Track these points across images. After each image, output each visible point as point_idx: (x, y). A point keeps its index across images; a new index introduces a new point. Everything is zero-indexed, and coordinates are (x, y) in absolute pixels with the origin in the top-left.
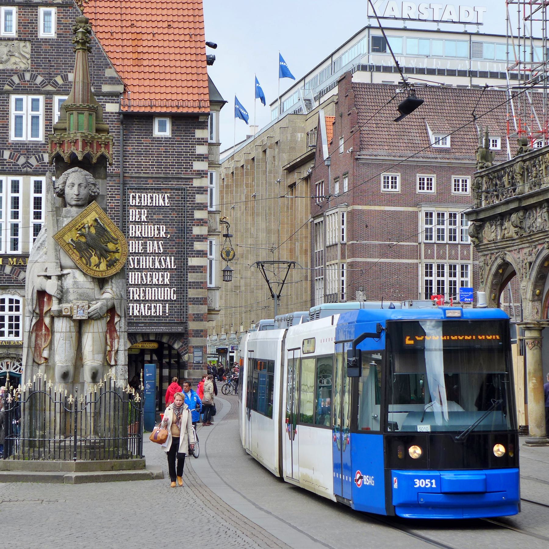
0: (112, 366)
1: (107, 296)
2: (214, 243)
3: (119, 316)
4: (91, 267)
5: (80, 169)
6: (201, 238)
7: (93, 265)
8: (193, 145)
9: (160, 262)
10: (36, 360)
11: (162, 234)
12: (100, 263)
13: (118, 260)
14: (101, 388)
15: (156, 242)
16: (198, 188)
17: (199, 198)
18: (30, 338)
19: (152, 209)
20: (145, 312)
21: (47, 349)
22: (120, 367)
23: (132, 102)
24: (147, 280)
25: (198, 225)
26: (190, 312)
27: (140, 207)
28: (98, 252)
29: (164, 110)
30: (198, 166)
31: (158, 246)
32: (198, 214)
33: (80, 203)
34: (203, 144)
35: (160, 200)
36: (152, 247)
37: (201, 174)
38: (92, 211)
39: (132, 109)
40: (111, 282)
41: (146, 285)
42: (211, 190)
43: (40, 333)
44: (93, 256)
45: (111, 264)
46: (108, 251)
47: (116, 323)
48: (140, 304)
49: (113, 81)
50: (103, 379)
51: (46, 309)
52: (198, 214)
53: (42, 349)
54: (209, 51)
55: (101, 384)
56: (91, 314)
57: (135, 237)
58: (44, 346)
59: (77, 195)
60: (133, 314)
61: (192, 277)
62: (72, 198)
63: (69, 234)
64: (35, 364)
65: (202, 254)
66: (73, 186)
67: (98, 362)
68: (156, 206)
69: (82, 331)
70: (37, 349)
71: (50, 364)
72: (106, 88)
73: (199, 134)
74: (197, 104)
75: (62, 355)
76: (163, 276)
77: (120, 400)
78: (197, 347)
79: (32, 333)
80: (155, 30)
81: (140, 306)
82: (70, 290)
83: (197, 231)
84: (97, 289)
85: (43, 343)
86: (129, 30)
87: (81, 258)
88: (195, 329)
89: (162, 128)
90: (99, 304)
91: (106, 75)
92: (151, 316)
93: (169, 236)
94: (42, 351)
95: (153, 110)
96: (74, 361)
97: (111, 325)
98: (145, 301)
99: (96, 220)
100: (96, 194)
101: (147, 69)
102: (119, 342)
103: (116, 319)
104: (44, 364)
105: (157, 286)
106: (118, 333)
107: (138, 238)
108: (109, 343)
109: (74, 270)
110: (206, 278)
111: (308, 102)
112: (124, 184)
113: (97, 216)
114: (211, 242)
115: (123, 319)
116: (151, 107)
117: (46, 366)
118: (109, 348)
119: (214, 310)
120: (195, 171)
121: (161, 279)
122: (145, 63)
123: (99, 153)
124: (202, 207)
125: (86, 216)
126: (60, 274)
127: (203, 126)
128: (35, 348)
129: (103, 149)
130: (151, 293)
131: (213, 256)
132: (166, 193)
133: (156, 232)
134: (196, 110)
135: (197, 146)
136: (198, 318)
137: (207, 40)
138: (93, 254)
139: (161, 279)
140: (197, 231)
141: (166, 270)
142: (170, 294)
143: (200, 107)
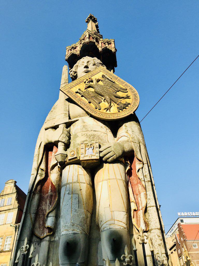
7: (102, 108)
10: (37, 232)
12: (110, 106)
21: (52, 214)
28: (107, 97)
50: (131, 247)
58: (48, 211)
67: (121, 224)
71: (57, 238)
79: (34, 194)
82: (78, 134)
84: (110, 134)
87: (90, 103)
94: (46, 218)
96: (86, 227)
99: (103, 76)
104: (48, 238)
117: (50, 242)
126: (67, 120)
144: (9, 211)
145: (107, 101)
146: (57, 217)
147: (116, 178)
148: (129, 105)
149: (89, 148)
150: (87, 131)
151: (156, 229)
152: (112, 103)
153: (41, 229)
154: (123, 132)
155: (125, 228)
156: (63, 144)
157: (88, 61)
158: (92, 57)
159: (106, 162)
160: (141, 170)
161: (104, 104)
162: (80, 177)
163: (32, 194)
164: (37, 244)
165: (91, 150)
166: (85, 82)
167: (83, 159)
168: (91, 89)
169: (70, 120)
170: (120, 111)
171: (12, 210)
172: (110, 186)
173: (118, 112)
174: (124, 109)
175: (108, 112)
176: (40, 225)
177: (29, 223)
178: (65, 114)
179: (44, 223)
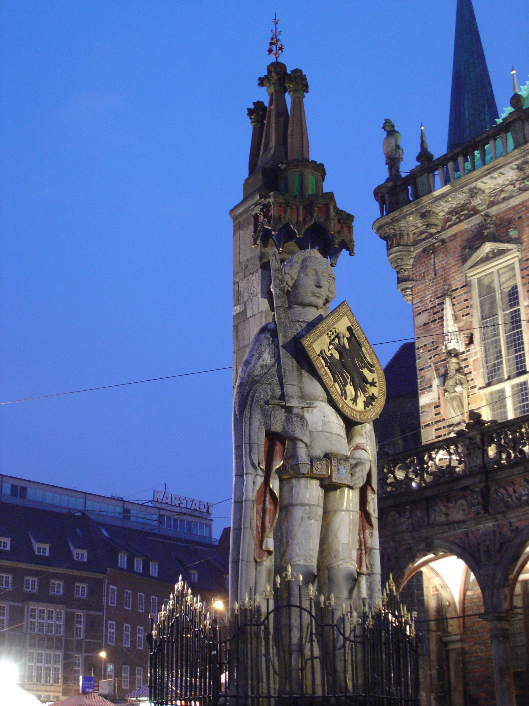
4: (347, 401)
13: (376, 398)
99: (349, 329)
102: (371, 534)
138: (349, 381)
161: (350, 389)
166: (330, 337)
170: (367, 409)
174: (370, 406)
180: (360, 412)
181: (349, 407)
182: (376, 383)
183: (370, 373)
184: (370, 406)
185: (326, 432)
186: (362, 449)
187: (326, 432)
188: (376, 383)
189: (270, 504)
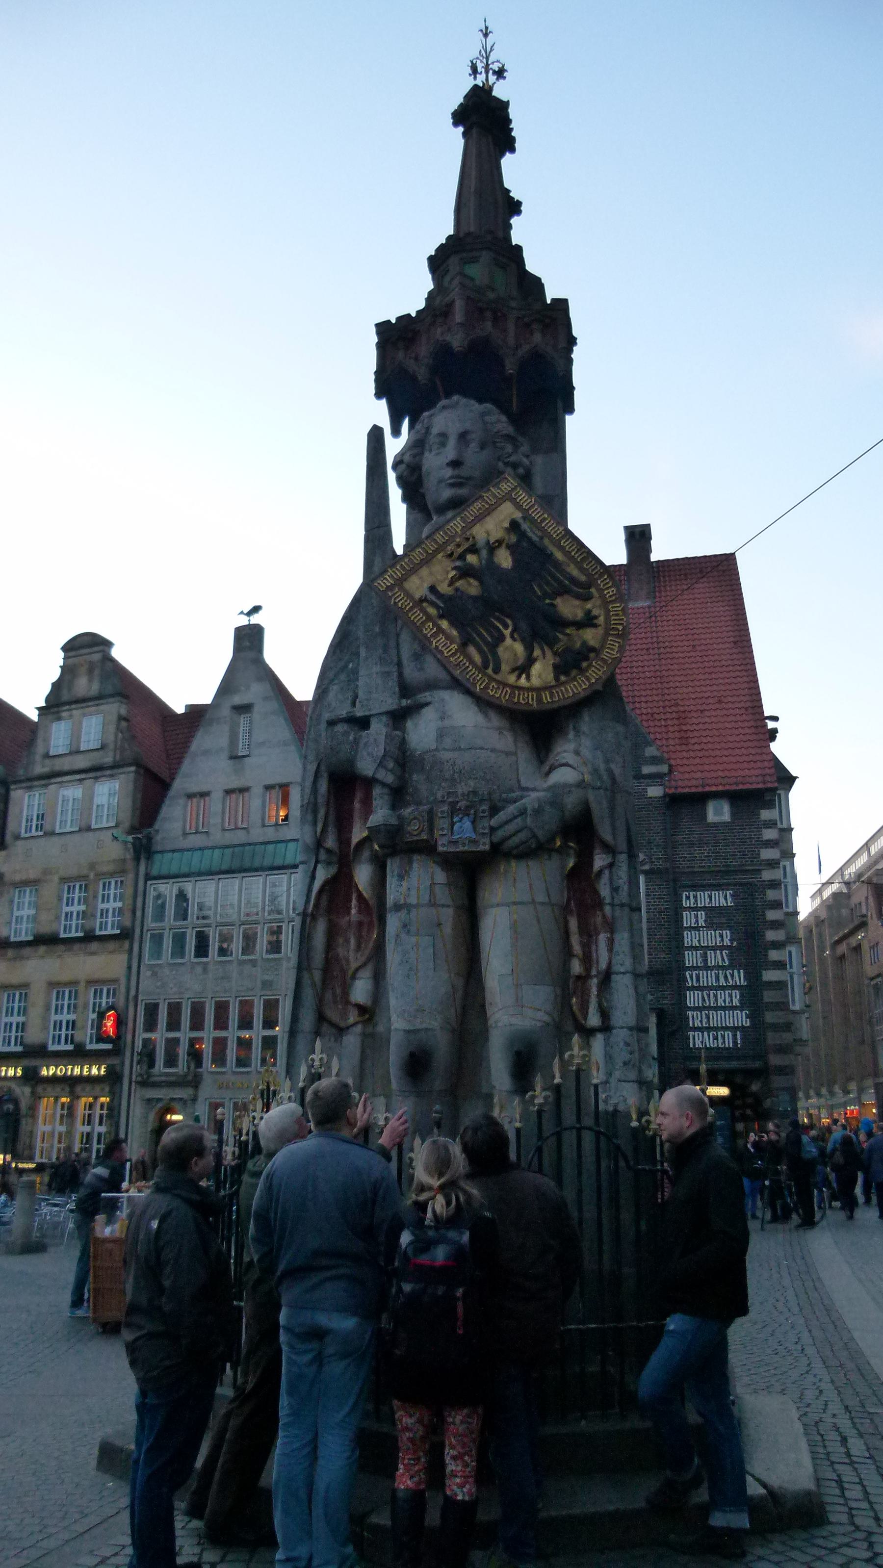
0: (588, 1033)
1: (563, 776)
2: (794, 954)
3: (609, 849)
4: (498, 677)
5: (464, 401)
6: (777, 945)
7: (505, 668)
8: (759, 829)
9: (726, 977)
11: (727, 942)
12: (530, 661)
13: (592, 649)
14: (540, 1113)
15: (718, 952)
16: (769, 881)
17: (771, 895)
18: (305, 938)
19: (711, 911)
20: (710, 1043)
22: (620, 1035)
23: (680, 783)
24: (709, 1000)
25: (772, 929)
26: (770, 1042)
27: (696, 909)
28: (523, 626)
29: (720, 788)
30: (767, 854)
31: (722, 957)
32: (772, 915)
33: (463, 492)
34: (771, 828)
35: (722, 899)
36: (714, 959)
37: (773, 864)
38: (500, 501)
39: (680, 790)
40: (575, 728)
41: (710, 1008)
42: (786, 886)
43: (343, 921)
44: (508, 641)
45: (570, 663)
46: (562, 623)
47: (600, 872)
48: (702, 1032)
49: (655, 760)
51: (358, 834)
52: (772, 915)
53: (350, 972)
54: (771, 725)
55: (540, 1095)
56: (500, 834)
57: (692, 947)
58: (354, 965)
59: (455, 464)
60: (694, 1045)
61: (769, 996)
62: (440, 481)
63: (424, 571)
64: (325, 1028)
65: (780, 965)
66: (443, 444)
68: (716, 907)
69: (479, 903)
70: (334, 976)
72: (646, 770)
73: (766, 815)
74: (760, 779)
75: (411, 991)
76: (731, 996)
77: (622, 1164)
78: (784, 1089)
79: (314, 917)
80: (705, 707)
81: (703, 1036)
83: (771, 935)
84: (524, 756)
85: (352, 955)
86: (674, 709)
88: (778, 1064)
89: (718, 812)
90: (531, 800)
91: (647, 755)
92: (718, 1048)
93: (735, 944)
95: (707, 789)
97: (580, 880)
98: (709, 1029)
99: (514, 526)
100: (521, 471)
101: (697, 747)
103: (599, 861)
104: (359, 1028)
105: (724, 1008)
106: (607, 909)
107: (696, 948)
108: (577, 948)
109: (445, 695)
110: (787, 996)
111: (847, 884)
112: (675, 880)
113: (518, 515)
114: (790, 953)
115: (623, 858)
116: (703, 786)
117: (364, 1035)
118: (576, 967)
119: (801, 1040)
120: (763, 860)
121: (728, 1000)
122: (692, 741)
123: (526, 348)
124: (777, 905)
125: (480, 518)
127: (770, 805)
128: (326, 970)
129: (537, 337)
130: (716, 1019)
131: (794, 970)
132: (728, 890)
133: (719, 939)
134: (761, 786)
135: (764, 831)
136: (782, 1050)
137: (766, 714)
138: (507, 633)
139: (728, 1000)
140: (771, 935)
141: (735, 987)
142: (741, 1019)
143: (764, 783)
144: (99, 774)
145: (523, 640)
146: (379, 977)
147: (533, 900)
148: (592, 655)
149: (460, 816)
150: (454, 750)
151: (622, 1028)
152: (536, 645)
153: (340, 1007)
154: (565, 751)
155: (548, 1024)
156: (386, 791)
157: (461, 430)
158: (480, 401)
159: (509, 855)
160: (607, 872)
161: (512, 648)
162: (437, 889)
163: (308, 919)
164: (332, 1039)
165: (467, 824)
166: (450, 555)
167: (445, 849)
168: (470, 584)
169: (404, 702)
170: (563, 678)
171: (108, 772)
172: (516, 921)
173: (553, 683)
174: (574, 672)
175: (523, 681)
176: (334, 994)
177: (309, 996)
178: (388, 674)
179: (346, 994)
180: (538, 690)
181: (505, 685)
182: (596, 617)
183: (577, 602)
184: (574, 672)
185: (444, 749)
186: (566, 765)
187: (444, 749)
188: (596, 617)
189: (360, 912)
